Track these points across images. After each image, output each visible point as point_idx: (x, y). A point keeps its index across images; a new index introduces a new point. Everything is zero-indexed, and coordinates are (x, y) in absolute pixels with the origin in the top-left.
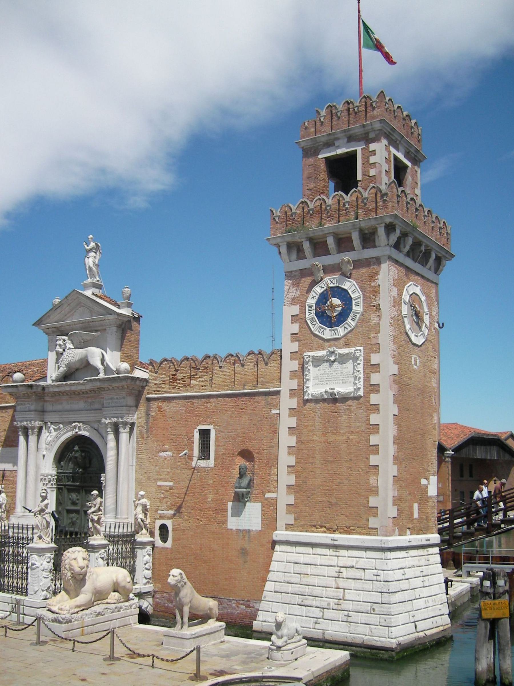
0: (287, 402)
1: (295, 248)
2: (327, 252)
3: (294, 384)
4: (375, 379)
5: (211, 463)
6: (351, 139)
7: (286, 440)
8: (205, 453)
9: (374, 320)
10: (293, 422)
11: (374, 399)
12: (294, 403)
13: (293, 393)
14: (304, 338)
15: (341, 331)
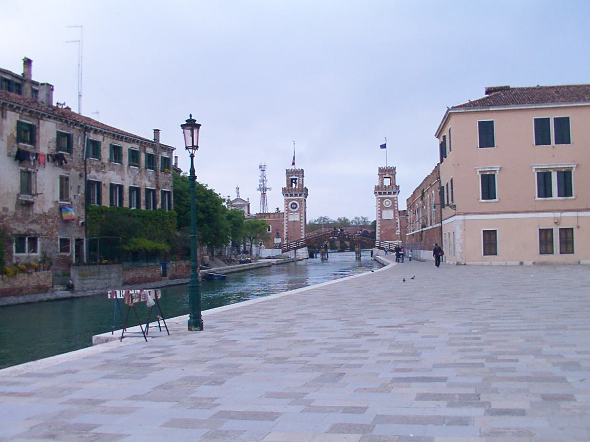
0: (286, 222)
1: (287, 195)
2: (293, 196)
3: (287, 218)
4: (301, 218)
5: (271, 232)
6: (296, 176)
7: (285, 228)
8: (269, 230)
9: (301, 209)
10: (287, 225)
11: (302, 221)
12: (287, 222)
13: (287, 220)
14: (288, 211)
15: (295, 210)
